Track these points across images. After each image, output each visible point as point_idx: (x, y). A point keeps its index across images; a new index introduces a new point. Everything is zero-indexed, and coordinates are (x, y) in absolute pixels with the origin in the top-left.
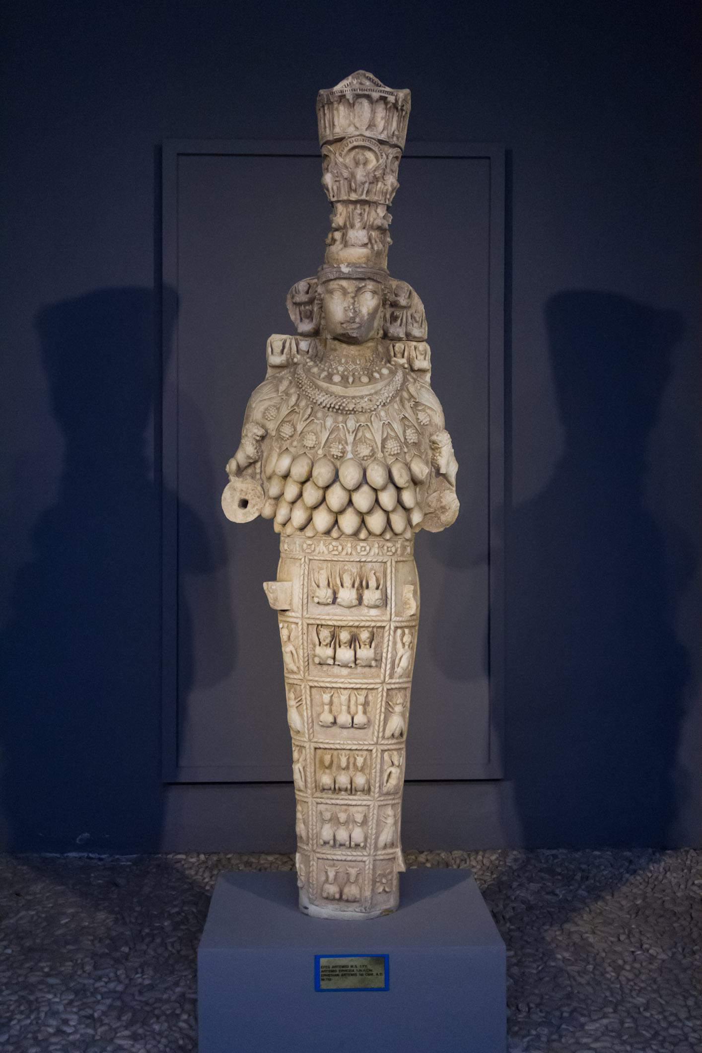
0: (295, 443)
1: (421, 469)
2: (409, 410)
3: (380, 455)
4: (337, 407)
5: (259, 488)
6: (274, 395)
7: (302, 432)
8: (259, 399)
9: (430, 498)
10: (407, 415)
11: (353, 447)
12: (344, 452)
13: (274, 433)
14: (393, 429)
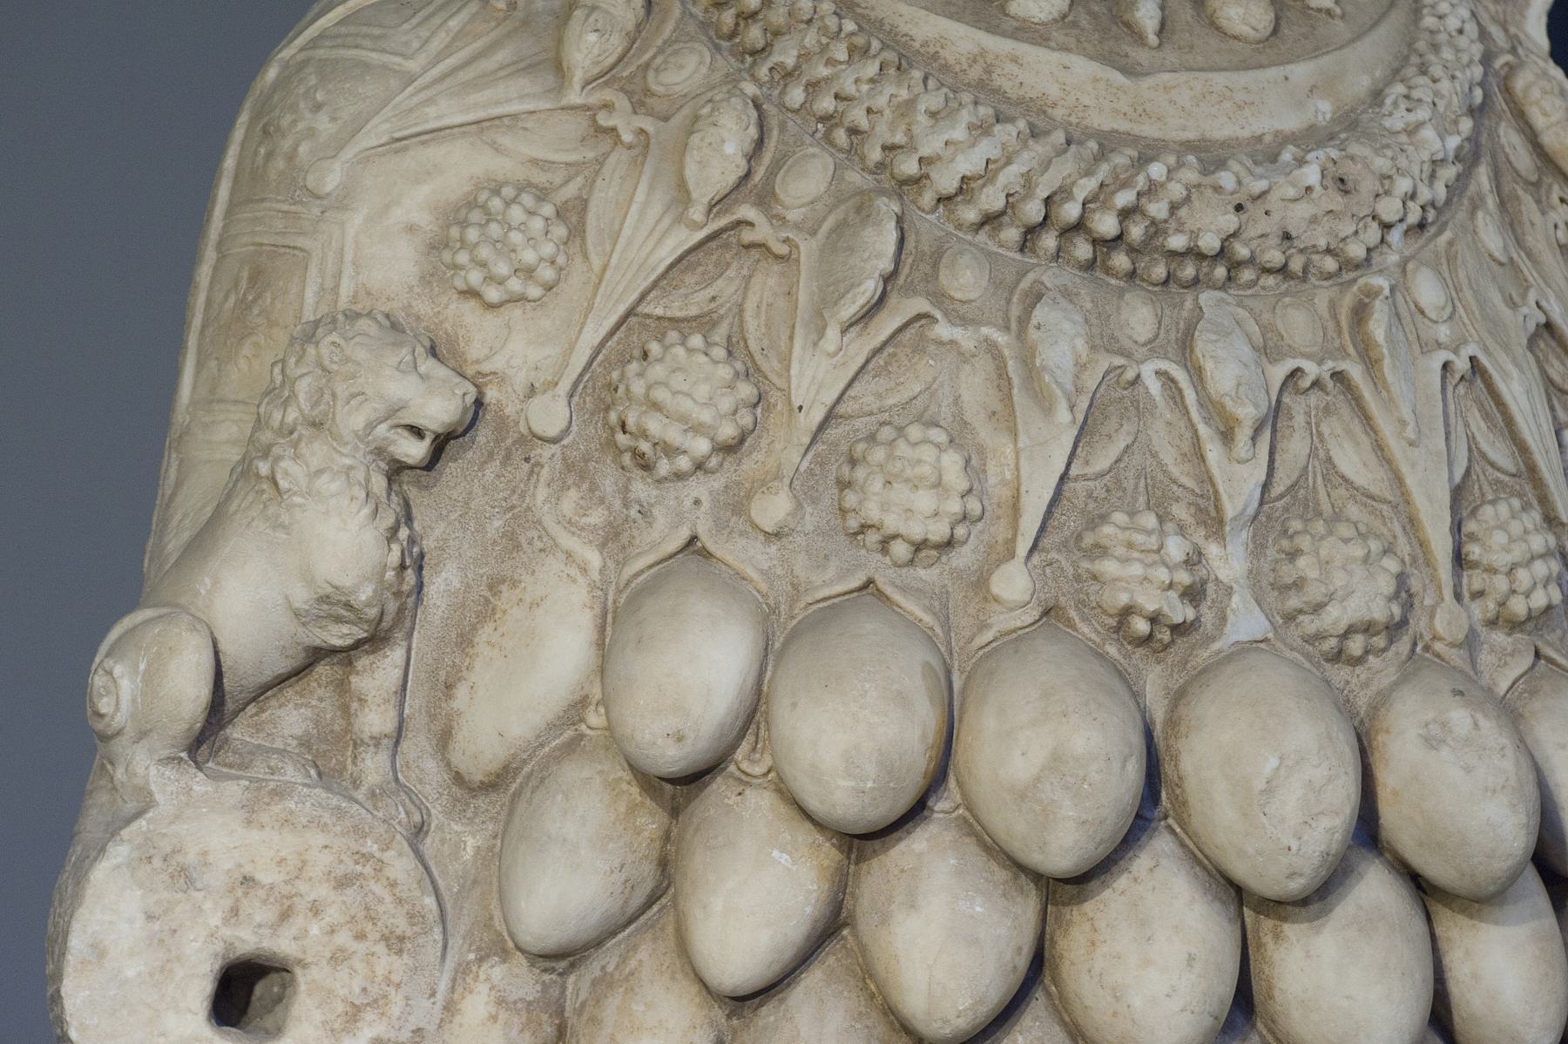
0: (774, 508)
5: (401, 865)
6: (516, 96)
7: (830, 417)
8: (377, 132)
11: (1257, 548)
13: (549, 415)
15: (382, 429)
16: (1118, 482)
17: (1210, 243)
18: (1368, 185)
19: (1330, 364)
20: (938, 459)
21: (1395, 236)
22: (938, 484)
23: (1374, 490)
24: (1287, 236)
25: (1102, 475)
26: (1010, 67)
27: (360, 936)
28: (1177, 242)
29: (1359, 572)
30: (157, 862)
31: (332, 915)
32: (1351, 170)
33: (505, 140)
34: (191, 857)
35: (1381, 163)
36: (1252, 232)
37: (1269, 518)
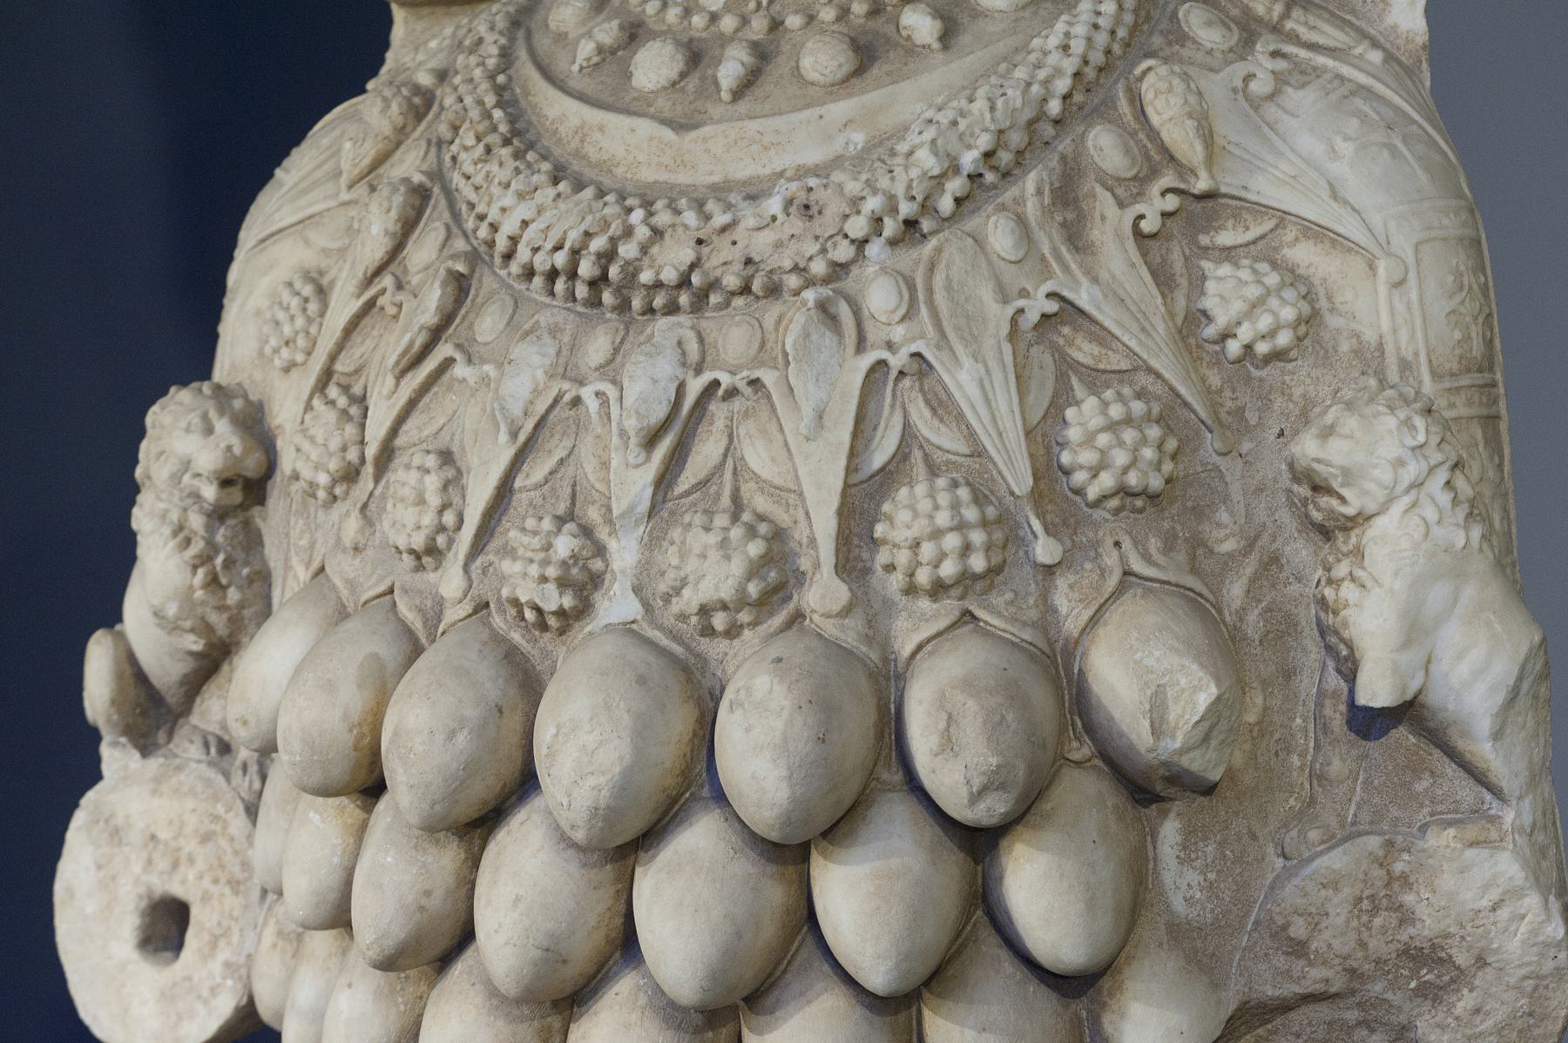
1: (1150, 680)
2: (1116, 255)
3: (823, 593)
4: (586, 268)
9: (1290, 894)
10: (1084, 297)
11: (653, 543)
12: (584, 584)
14: (942, 405)
15: (186, 478)
16: (553, 489)
17: (669, 276)
18: (834, 207)
19: (745, 373)
20: (421, 481)
21: (875, 249)
22: (421, 501)
23: (778, 481)
24: (749, 261)
25: (538, 486)
26: (597, 135)
27: (216, 881)
28: (646, 277)
29: (714, 556)
30: (102, 824)
31: (200, 864)
32: (821, 195)
33: (311, 235)
34: (119, 820)
35: (853, 187)
36: (713, 262)
37: (672, 513)
